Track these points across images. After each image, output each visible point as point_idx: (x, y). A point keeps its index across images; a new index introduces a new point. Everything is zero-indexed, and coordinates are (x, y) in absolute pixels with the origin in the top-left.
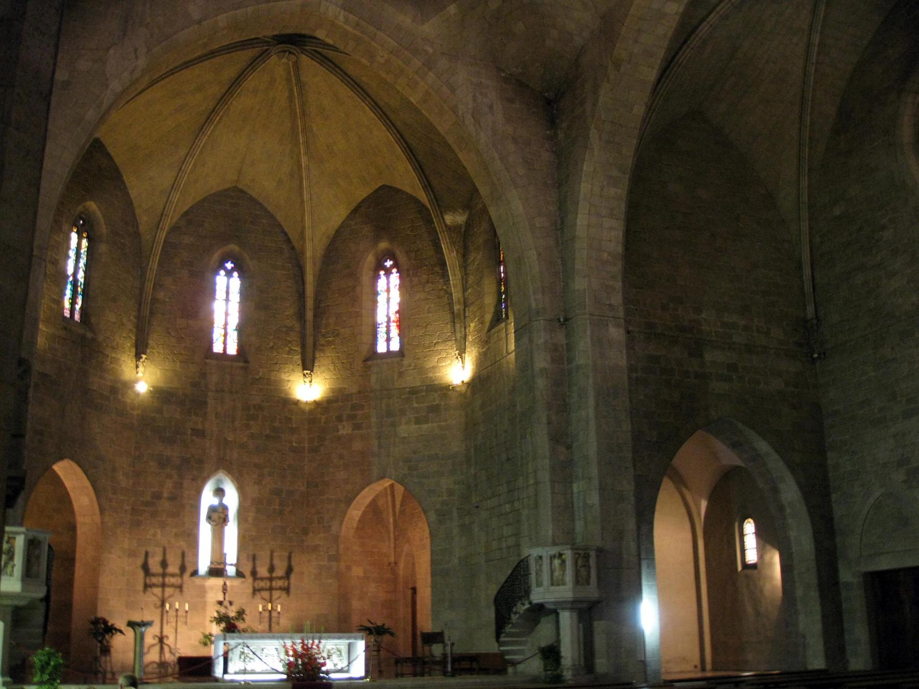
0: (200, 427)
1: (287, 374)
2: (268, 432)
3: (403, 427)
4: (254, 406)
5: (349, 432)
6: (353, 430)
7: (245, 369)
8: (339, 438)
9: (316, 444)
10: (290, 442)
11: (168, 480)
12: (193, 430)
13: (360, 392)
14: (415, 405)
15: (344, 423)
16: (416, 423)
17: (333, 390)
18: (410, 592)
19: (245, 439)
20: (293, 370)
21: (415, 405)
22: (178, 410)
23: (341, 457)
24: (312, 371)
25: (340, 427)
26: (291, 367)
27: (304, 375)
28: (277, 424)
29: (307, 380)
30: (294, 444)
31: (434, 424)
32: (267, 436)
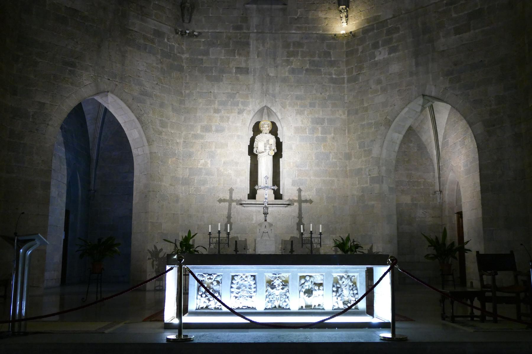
0: (243, 65)
1: (324, 13)
2: (308, 66)
3: (443, 40)
4: (294, 43)
5: (386, 56)
6: (389, 54)
7: (284, 10)
8: (376, 64)
9: (355, 73)
10: (330, 74)
11: (216, 115)
12: (237, 68)
13: (394, 17)
14: (454, 15)
15: (380, 49)
16: (456, 34)
17: (368, 20)
18: (455, 217)
19: (287, 74)
20: (329, 9)
21: (454, 15)
22: (223, 51)
23: (379, 82)
24: (348, 6)
25: (377, 53)
26: (327, 5)
27: (341, 11)
28: (316, 59)
29: (343, 15)
30: (334, 76)
31: (477, 31)
32: (307, 70)
